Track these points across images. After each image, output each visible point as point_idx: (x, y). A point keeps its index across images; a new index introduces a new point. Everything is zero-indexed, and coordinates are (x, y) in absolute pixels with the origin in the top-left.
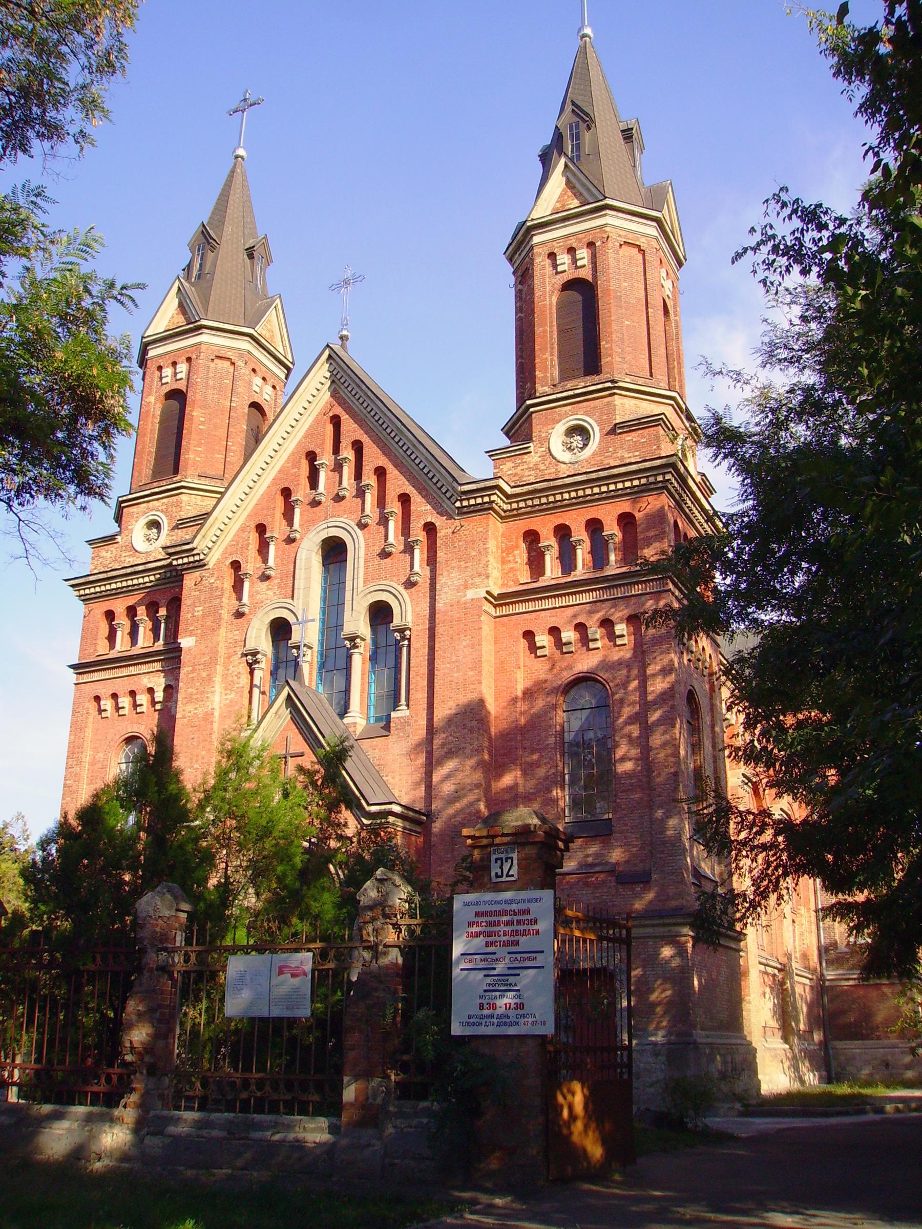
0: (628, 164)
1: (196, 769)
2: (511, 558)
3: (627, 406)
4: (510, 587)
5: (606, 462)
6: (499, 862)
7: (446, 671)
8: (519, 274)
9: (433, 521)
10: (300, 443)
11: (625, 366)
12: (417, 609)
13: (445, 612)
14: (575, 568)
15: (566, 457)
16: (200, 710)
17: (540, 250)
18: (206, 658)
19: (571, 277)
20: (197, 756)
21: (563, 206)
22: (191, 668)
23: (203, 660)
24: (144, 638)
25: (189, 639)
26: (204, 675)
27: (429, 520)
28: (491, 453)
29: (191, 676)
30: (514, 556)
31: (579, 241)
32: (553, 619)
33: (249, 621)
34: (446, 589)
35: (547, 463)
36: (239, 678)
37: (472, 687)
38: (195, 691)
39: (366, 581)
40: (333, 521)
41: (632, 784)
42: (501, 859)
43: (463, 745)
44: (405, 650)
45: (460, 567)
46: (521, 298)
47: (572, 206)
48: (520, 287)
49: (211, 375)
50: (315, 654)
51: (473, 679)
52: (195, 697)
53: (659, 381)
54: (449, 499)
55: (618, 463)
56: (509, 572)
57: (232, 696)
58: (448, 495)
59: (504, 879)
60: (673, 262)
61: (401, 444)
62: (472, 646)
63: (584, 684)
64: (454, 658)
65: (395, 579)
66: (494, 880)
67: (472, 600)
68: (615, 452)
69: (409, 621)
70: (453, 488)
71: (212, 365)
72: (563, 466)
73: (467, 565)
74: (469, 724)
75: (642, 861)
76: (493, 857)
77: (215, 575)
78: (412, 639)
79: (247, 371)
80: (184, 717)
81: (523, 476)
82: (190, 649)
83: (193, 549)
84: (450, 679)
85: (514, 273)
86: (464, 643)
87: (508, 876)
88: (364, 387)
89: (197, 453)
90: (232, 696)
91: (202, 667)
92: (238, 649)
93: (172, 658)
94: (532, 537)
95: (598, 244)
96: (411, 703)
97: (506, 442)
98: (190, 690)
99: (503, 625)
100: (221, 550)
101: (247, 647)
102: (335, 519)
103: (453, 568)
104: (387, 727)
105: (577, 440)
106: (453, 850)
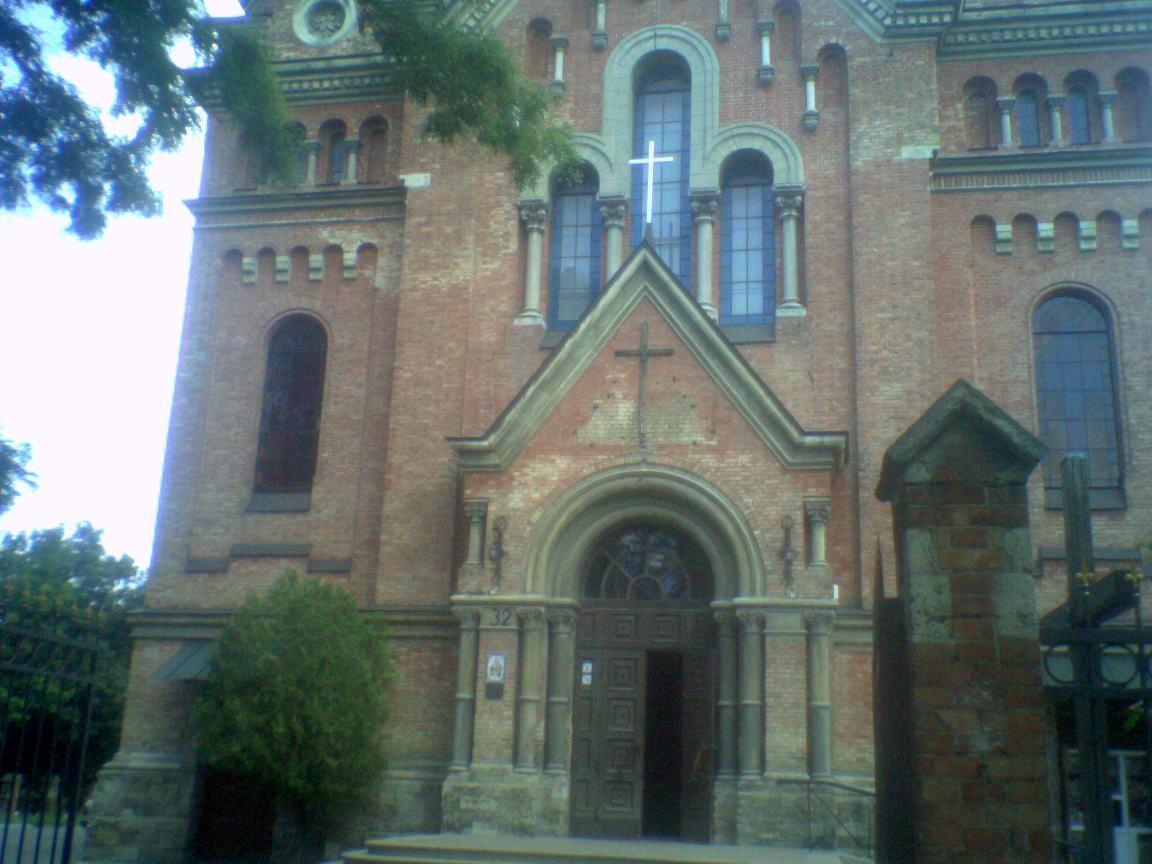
1: (440, 367)
2: (950, 112)
9: (840, 42)
12: (812, 167)
16: (444, 281)
18: (451, 206)
22: (423, 219)
26: (449, 230)
27: (833, 41)
29: (425, 229)
30: (956, 110)
32: (1024, 204)
34: (866, 141)
36: (508, 241)
37: (917, 283)
39: (724, 118)
40: (664, 28)
43: (908, 364)
44: (790, 228)
45: (888, 113)
52: (434, 261)
54: (872, 13)
56: (949, 131)
64: (886, 240)
69: (800, 178)
73: (899, 110)
74: (915, 335)
78: (807, 208)
82: (420, 192)
84: (878, 268)
86: (902, 221)
94: (981, 89)
96: (809, 299)
102: (667, 25)
104: (773, 333)
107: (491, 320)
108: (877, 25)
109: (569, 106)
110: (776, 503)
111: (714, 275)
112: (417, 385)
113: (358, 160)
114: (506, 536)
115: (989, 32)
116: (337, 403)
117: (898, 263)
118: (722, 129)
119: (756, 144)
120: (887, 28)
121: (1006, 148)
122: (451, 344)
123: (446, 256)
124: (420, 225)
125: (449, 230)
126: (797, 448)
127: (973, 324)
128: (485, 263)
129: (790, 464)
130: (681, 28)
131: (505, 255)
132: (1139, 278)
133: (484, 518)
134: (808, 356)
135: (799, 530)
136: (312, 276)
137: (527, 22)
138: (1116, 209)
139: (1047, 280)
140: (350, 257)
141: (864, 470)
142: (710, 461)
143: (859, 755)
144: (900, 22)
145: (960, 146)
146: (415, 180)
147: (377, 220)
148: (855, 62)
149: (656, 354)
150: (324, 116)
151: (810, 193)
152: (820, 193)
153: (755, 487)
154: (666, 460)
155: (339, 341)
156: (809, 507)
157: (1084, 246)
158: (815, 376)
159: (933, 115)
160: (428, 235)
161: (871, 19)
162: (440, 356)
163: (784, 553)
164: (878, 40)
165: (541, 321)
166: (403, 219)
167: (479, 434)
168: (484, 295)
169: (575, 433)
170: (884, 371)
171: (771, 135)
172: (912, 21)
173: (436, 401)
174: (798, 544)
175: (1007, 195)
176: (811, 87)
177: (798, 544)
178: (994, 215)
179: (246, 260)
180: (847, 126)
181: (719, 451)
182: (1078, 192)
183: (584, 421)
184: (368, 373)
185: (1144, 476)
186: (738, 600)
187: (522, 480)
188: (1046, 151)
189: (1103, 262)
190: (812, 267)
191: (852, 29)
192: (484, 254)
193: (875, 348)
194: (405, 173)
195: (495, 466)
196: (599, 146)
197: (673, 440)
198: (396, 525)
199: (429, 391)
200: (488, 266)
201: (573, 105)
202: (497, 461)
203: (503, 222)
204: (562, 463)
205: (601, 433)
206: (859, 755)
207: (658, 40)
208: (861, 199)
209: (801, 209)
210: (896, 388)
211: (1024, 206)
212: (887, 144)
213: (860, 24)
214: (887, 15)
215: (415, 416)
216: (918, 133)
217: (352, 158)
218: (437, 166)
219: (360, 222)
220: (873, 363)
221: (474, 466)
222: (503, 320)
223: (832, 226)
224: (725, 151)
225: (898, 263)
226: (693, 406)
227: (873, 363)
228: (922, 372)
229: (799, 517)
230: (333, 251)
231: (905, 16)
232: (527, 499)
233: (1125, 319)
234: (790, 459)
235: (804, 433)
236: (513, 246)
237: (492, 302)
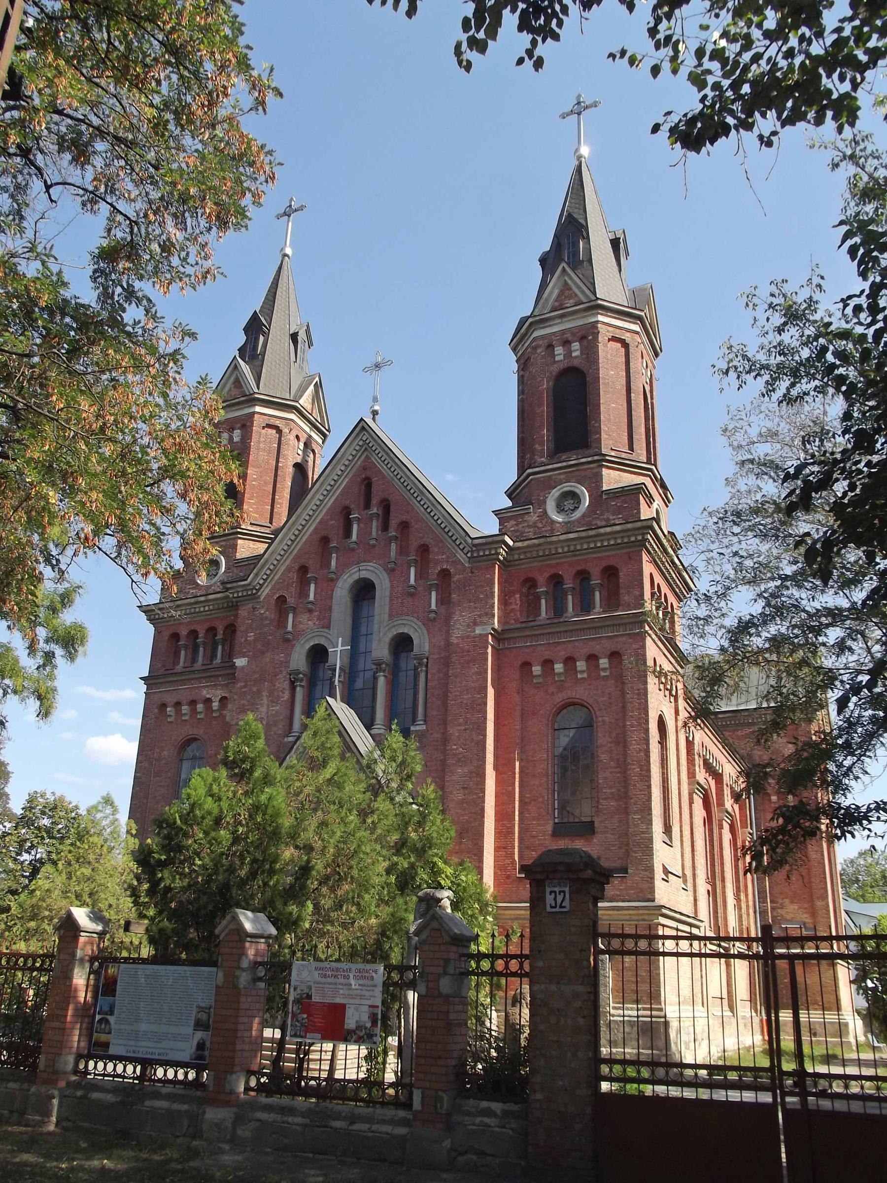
0: (616, 268)
2: (512, 600)
3: (612, 476)
5: (594, 522)
6: (553, 895)
7: (457, 693)
8: (522, 361)
10: (336, 500)
11: (611, 442)
14: (567, 608)
15: (559, 518)
18: (257, 676)
21: (561, 305)
22: (243, 684)
24: (204, 656)
25: (243, 659)
26: (255, 689)
28: (497, 513)
30: (515, 599)
31: (573, 334)
32: (547, 653)
33: (293, 646)
39: (391, 616)
41: (612, 793)
42: (555, 892)
45: (469, 607)
46: (523, 383)
47: (568, 305)
48: (521, 373)
49: (262, 439)
50: (347, 675)
53: (639, 455)
54: (462, 550)
55: (604, 523)
58: (461, 546)
59: (558, 909)
60: (651, 353)
61: (422, 503)
63: (572, 707)
65: (415, 615)
66: (549, 909)
67: (480, 635)
68: (602, 514)
70: (465, 541)
71: (263, 431)
72: (558, 525)
75: (620, 858)
76: (548, 890)
77: (266, 607)
79: (292, 437)
81: (524, 532)
82: (243, 668)
83: (249, 585)
84: (460, 700)
85: (517, 361)
87: (561, 907)
88: (392, 455)
89: (250, 505)
91: (251, 683)
92: (283, 669)
93: (229, 674)
97: (509, 503)
98: (243, 702)
100: (269, 588)
105: (568, 504)
106: (461, 843)
109: (316, 614)
111: (386, 706)
119: (406, 630)
124: (242, 687)
125: (255, 689)
130: (371, 566)
136: (199, 717)
138: (596, 653)
139: (559, 698)
140: (215, 705)
144: (475, 555)
145: (516, 620)
146: (240, 662)
148: (455, 579)
150: (207, 625)
152: (436, 656)
157: (579, 676)
158: (428, 764)
171: (414, 625)
172: (481, 554)
175: (539, 648)
176: (434, 594)
179: (168, 709)
180: (448, 617)
182: (577, 644)
189: (590, 685)
192: (272, 701)
196: (328, 636)
203: (283, 684)
211: (547, 655)
219: (221, 685)
223: (441, 675)
224: (390, 635)
227: (455, 755)
230: (208, 701)
236: (286, 696)
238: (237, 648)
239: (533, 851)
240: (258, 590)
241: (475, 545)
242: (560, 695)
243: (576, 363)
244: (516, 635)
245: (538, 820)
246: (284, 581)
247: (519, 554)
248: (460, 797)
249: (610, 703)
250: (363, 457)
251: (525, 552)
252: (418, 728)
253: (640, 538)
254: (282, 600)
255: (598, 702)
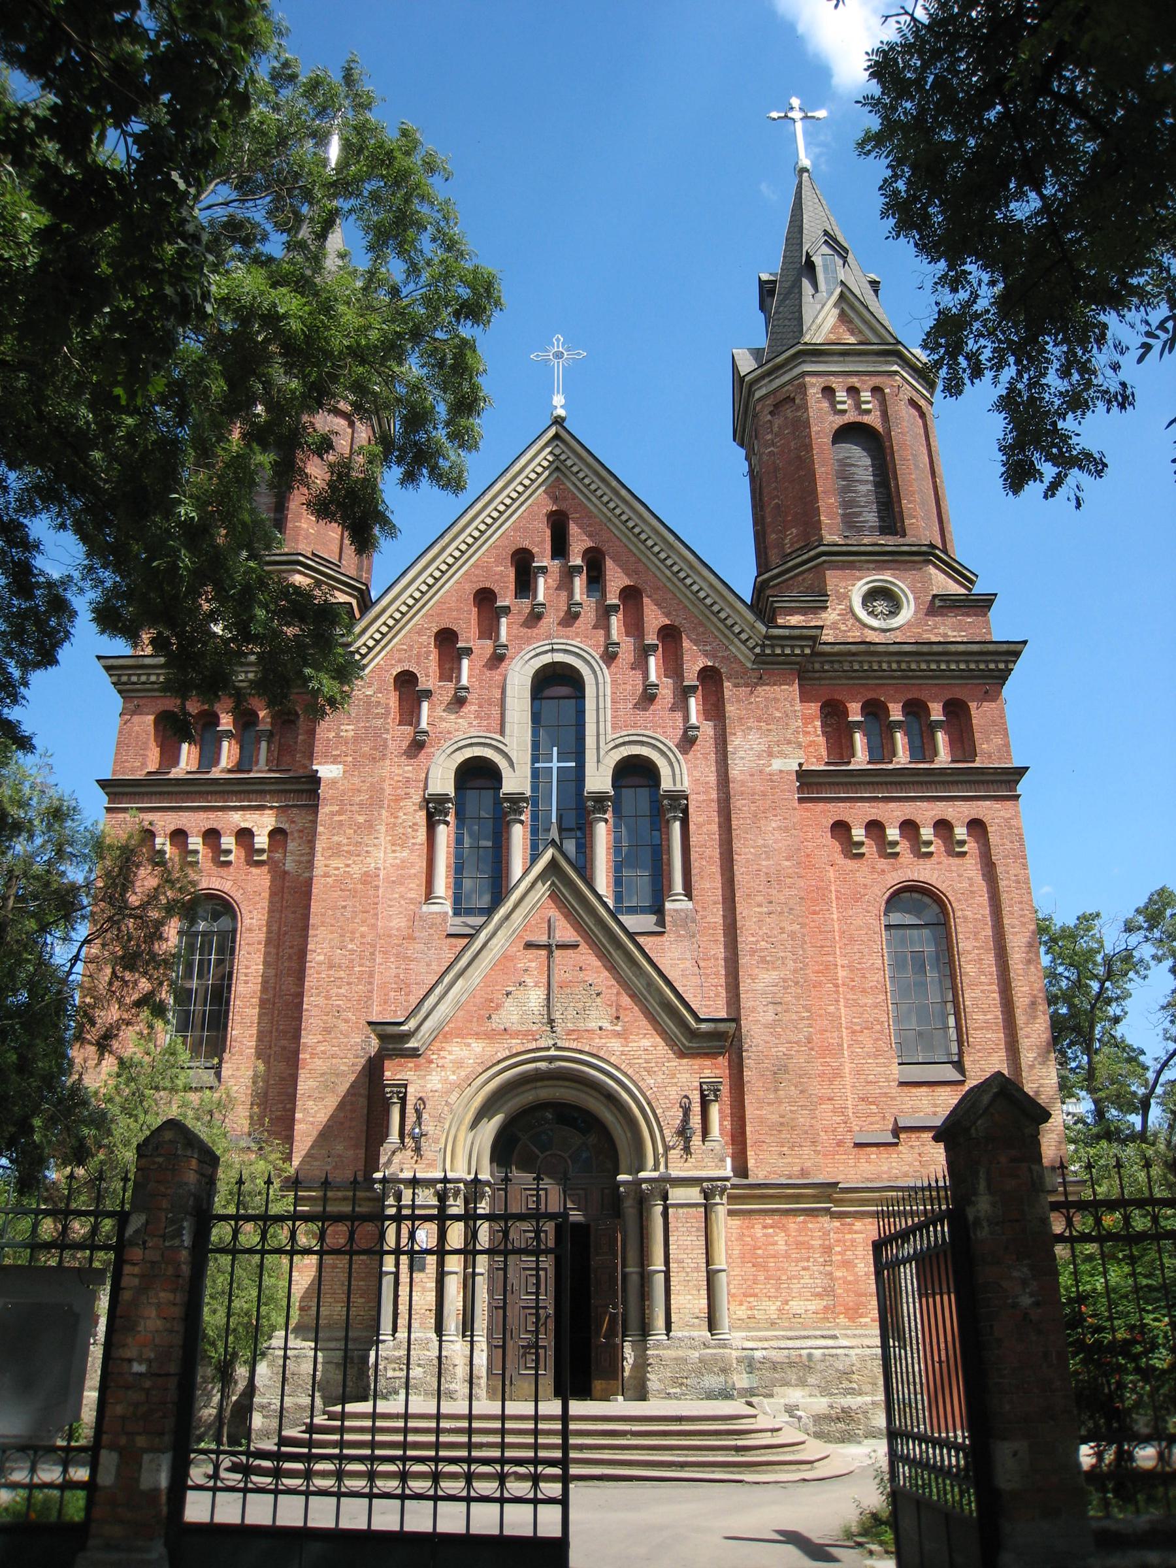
1: (352, 952)
2: (810, 729)
4: (812, 764)
13: (743, 783)
17: (813, 380)
18: (364, 797)
19: (852, 419)
20: (353, 933)
23: (357, 799)
24: (229, 758)
25: (333, 767)
26: (361, 819)
30: (815, 727)
32: (873, 810)
33: (430, 756)
34: (742, 754)
35: (850, 623)
36: (417, 831)
37: (788, 881)
38: (345, 841)
39: (615, 727)
43: (782, 954)
51: (790, 871)
52: (345, 848)
54: (744, 642)
57: (405, 854)
58: (744, 636)
62: (786, 829)
64: (760, 842)
67: (781, 771)
69: (685, 784)
78: (691, 810)
80: (326, 875)
82: (334, 782)
84: (755, 867)
86: (774, 825)
88: (614, 483)
90: (405, 854)
95: (887, 391)
96: (694, 893)
98: (336, 838)
99: (807, 810)
101: (431, 790)
103: (750, 728)
104: (661, 922)
105: (881, 606)
106: (776, 1090)
107: (401, 906)
108: (747, 651)
109: (474, 708)
110: (675, 1084)
112: (331, 967)
113: (269, 750)
114: (425, 1116)
115: (840, 662)
116: (246, 982)
117: (771, 862)
118: (615, 736)
120: (757, 655)
121: (858, 763)
122: (363, 929)
123: (358, 844)
124: (333, 814)
125: (361, 819)
126: (693, 1034)
127: (835, 917)
128: (394, 851)
129: (689, 1048)
131: (414, 844)
132: (969, 879)
133: (403, 1101)
134: (696, 946)
135: (696, 1108)
137: (435, 630)
141: (747, 1051)
142: (615, 1044)
143: (749, 1312)
144: (768, 651)
147: (287, 806)
149: (562, 947)
151: (691, 797)
152: (702, 797)
153: (656, 1069)
154: (574, 1045)
155: (247, 922)
156: (705, 1087)
158: (702, 964)
159: (798, 733)
160: (340, 822)
161: (743, 647)
162: (352, 940)
163: (683, 1132)
164: (749, 665)
165: (448, 908)
166: (317, 806)
167: (402, 1020)
168: (393, 882)
169: (489, 1018)
170: (763, 960)
173: (349, 984)
174: (695, 1121)
177: (695, 1121)
178: (849, 820)
181: (622, 1035)
183: (498, 1007)
184: (277, 954)
185: (979, 1051)
186: (642, 1175)
187: (441, 1062)
188: (890, 766)
189: (939, 863)
190: (696, 864)
191: (726, 654)
193: (754, 939)
194: (319, 764)
195: (417, 1049)
197: (582, 1026)
198: (311, 1103)
199: (342, 974)
200: (398, 854)
201: (476, 708)
202: (416, 1045)
204: (477, 1046)
205: (515, 1018)
206: (749, 1312)
207: (555, 654)
208: (739, 804)
209: (685, 811)
210: (774, 975)
212: (759, 757)
213: (734, 650)
214: (757, 645)
215: (328, 998)
216: (784, 747)
217: (264, 745)
218: (350, 759)
220: (753, 952)
221: (394, 1049)
222: (412, 907)
225: (771, 862)
226: (598, 994)
227: (753, 952)
228: (795, 961)
229: (696, 1097)
231: (772, 646)
232: (445, 1081)
233: (959, 914)
234: (687, 1044)
235: (699, 1020)
237: (402, 889)
238: (319, 748)
239: (871, 1103)
240: (364, 656)
241: (767, 637)
242: (894, 874)
243: (866, 419)
244: (821, 780)
245: (876, 1057)
246: (411, 647)
247: (822, 663)
248: (770, 1016)
249: (971, 892)
250: (552, 479)
251: (832, 662)
252: (677, 905)
253: (1001, 666)
254: (406, 681)
255: (954, 890)
